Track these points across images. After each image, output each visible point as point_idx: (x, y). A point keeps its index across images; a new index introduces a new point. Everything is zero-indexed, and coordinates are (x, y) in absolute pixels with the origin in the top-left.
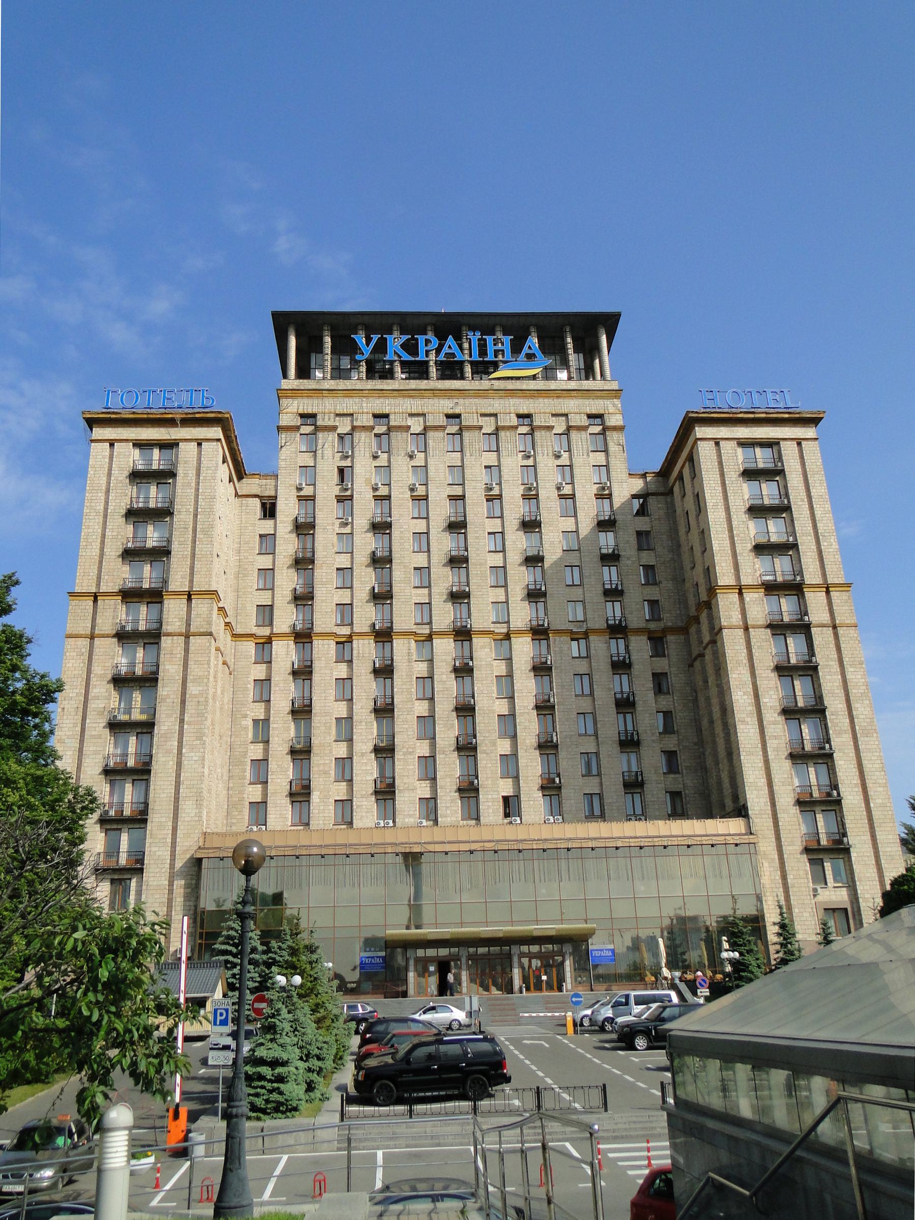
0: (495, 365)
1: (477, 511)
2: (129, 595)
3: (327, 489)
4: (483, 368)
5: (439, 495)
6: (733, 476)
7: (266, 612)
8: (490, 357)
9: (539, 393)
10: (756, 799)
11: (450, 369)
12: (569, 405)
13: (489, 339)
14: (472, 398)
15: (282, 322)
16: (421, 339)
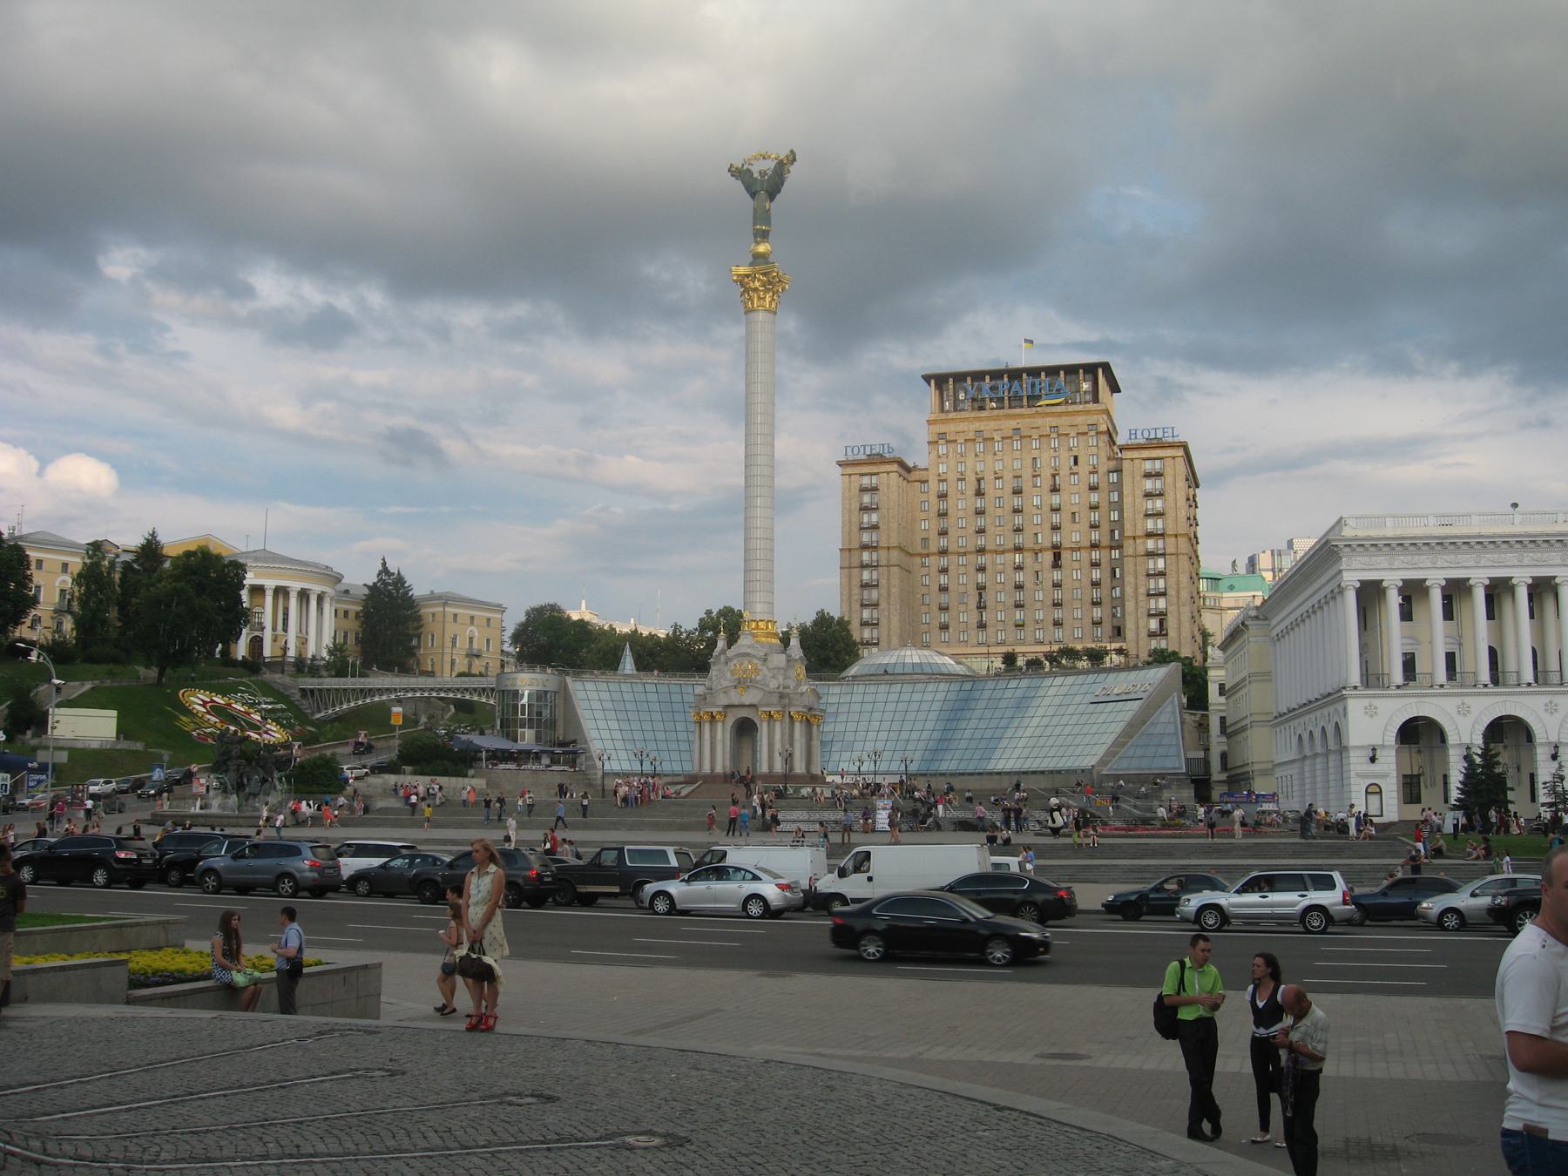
0: (1039, 398)
1: (1027, 486)
2: (865, 547)
3: (952, 477)
4: (1033, 399)
5: (1008, 476)
6: (1138, 478)
7: (925, 540)
8: (1037, 392)
9: (1060, 414)
10: (1129, 633)
11: (1016, 400)
12: (1079, 419)
13: (1037, 381)
14: (1023, 418)
15: (927, 378)
16: (1000, 383)
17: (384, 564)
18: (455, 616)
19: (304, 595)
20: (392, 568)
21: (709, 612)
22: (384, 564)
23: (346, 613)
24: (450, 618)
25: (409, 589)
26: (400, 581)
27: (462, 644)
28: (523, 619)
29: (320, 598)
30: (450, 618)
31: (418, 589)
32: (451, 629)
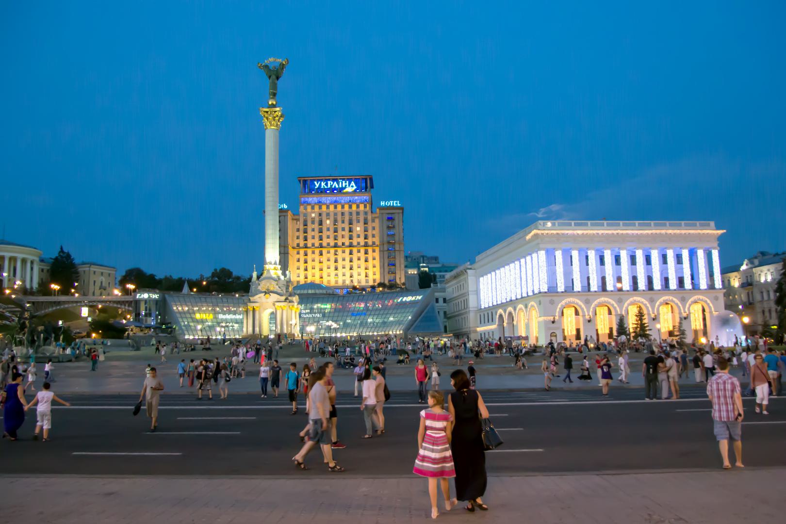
17: (62, 248)
18: (95, 272)
19: (24, 261)
20: (65, 250)
21: (216, 270)
22: (62, 248)
23: (42, 270)
24: (92, 273)
25: (73, 259)
26: (68, 256)
27: (98, 284)
28: (124, 274)
29: (32, 262)
30: (92, 273)
31: (77, 261)
32: (93, 278)
